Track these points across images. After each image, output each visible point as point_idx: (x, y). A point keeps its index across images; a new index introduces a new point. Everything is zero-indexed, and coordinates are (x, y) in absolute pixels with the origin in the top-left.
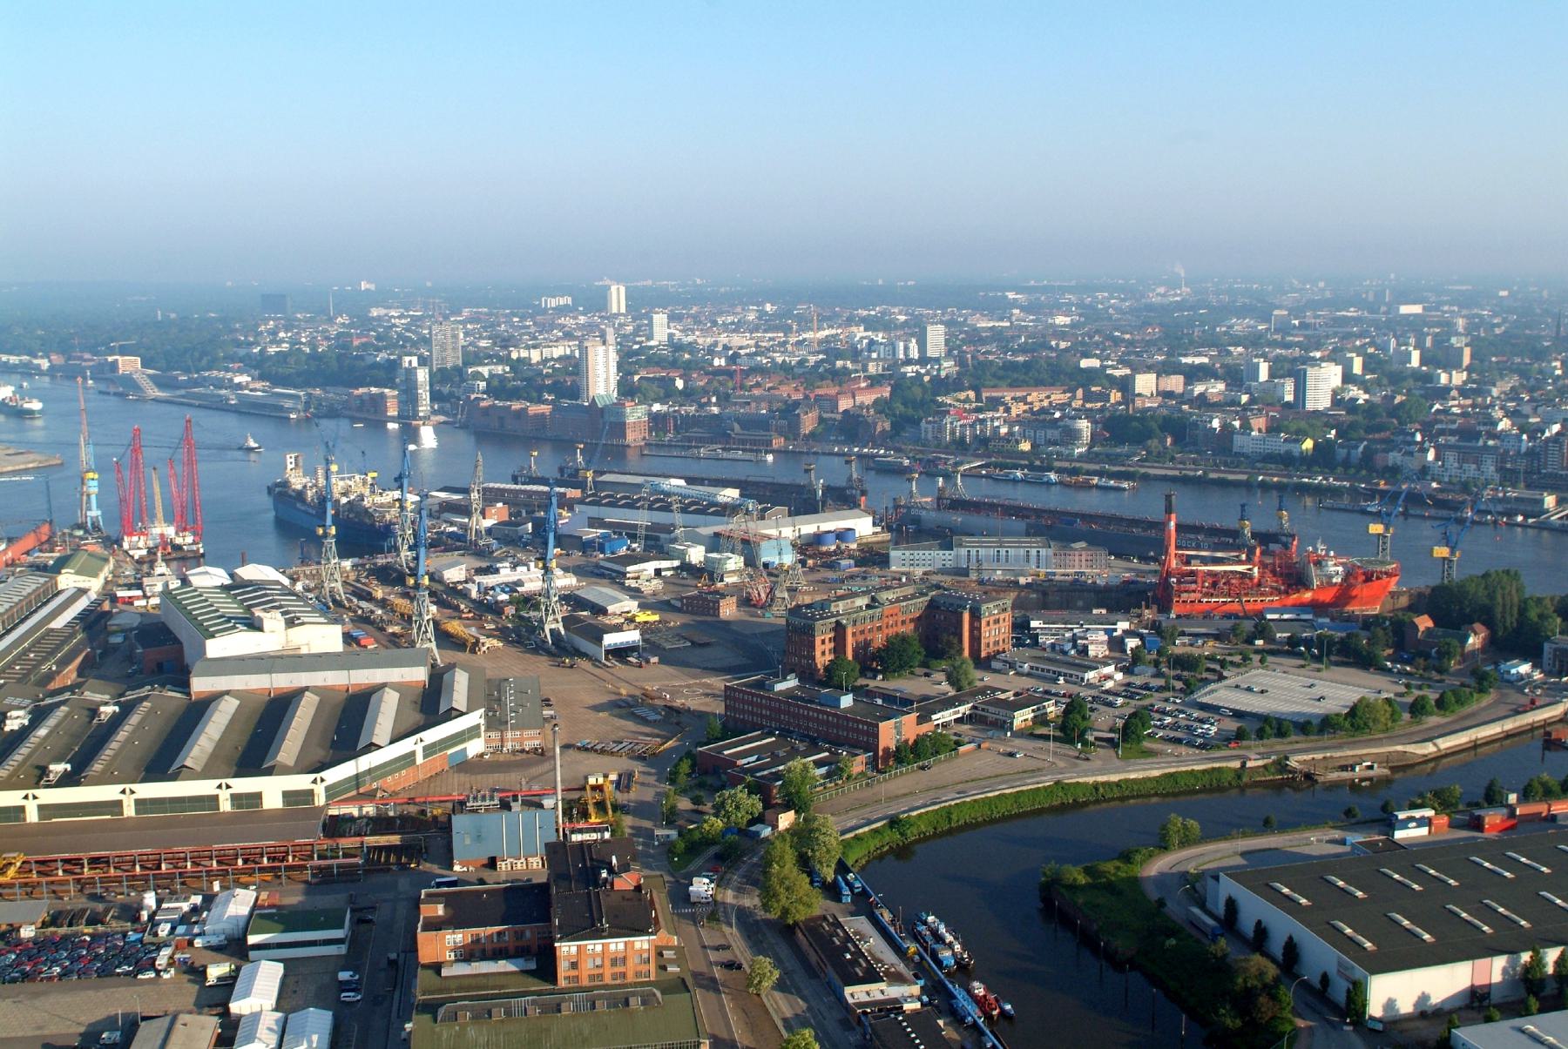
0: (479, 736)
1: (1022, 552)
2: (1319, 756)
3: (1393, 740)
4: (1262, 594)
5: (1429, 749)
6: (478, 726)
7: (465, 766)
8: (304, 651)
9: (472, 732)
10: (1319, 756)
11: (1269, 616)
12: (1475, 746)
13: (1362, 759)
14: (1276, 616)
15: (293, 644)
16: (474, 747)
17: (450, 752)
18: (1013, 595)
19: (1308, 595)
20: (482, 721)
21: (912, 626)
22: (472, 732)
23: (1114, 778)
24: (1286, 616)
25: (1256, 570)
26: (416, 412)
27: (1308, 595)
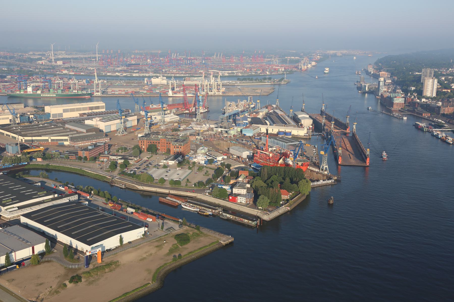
1: (282, 143)
4: (270, 162)
7: (63, 146)
16: (66, 143)
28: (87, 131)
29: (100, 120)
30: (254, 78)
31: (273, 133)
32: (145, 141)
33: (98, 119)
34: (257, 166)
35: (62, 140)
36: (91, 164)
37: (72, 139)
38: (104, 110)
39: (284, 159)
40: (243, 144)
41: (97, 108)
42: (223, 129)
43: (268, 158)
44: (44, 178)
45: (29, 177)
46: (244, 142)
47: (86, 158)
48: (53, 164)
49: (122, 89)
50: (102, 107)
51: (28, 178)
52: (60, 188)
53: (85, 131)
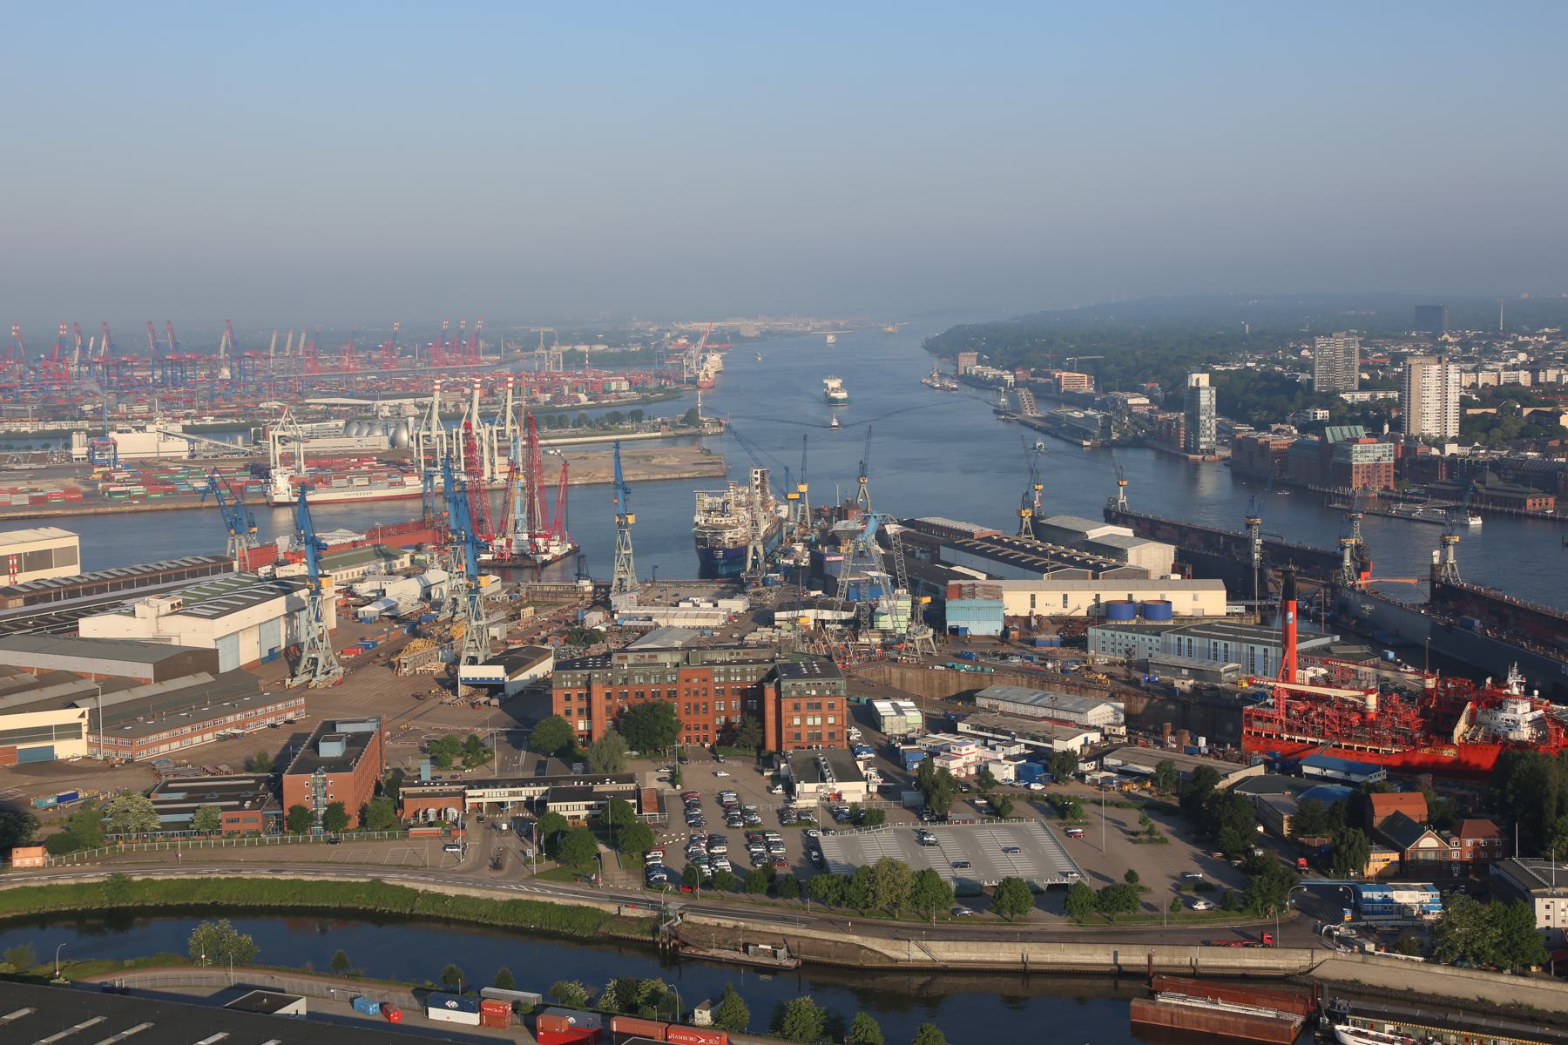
0: (79, 736)
1: (1245, 647)
2: (729, 923)
3: (861, 928)
5: (912, 952)
6: (79, 726)
7: (47, 766)
8: (175, 642)
9: (71, 731)
10: (729, 923)
11: (1306, 769)
12: (1024, 973)
13: (764, 936)
14: (1315, 771)
15: (163, 634)
16: (68, 750)
17: (20, 747)
18: (1140, 705)
19: (1449, 753)
20: (84, 721)
21: (736, 704)
22: (71, 731)
23: (451, 891)
24: (1329, 772)
25: (1372, 701)
26: (1197, 444)
27: (1449, 753)
28: (161, 675)
29: (176, 610)
30: (572, 416)
31: (1066, 612)
32: (596, 687)
33: (165, 605)
34: (1350, 768)
35: (44, 733)
36: (390, 850)
37: (106, 722)
38: (73, 571)
39: (1473, 714)
40: (1019, 671)
41: (40, 559)
42: (827, 615)
43: (1355, 719)
44: (240, 963)
45: (119, 968)
46: (1016, 661)
47: (335, 816)
48: (161, 872)
49: (22, 486)
50: (66, 556)
51: (120, 980)
52: (435, 1014)
53: (146, 671)
